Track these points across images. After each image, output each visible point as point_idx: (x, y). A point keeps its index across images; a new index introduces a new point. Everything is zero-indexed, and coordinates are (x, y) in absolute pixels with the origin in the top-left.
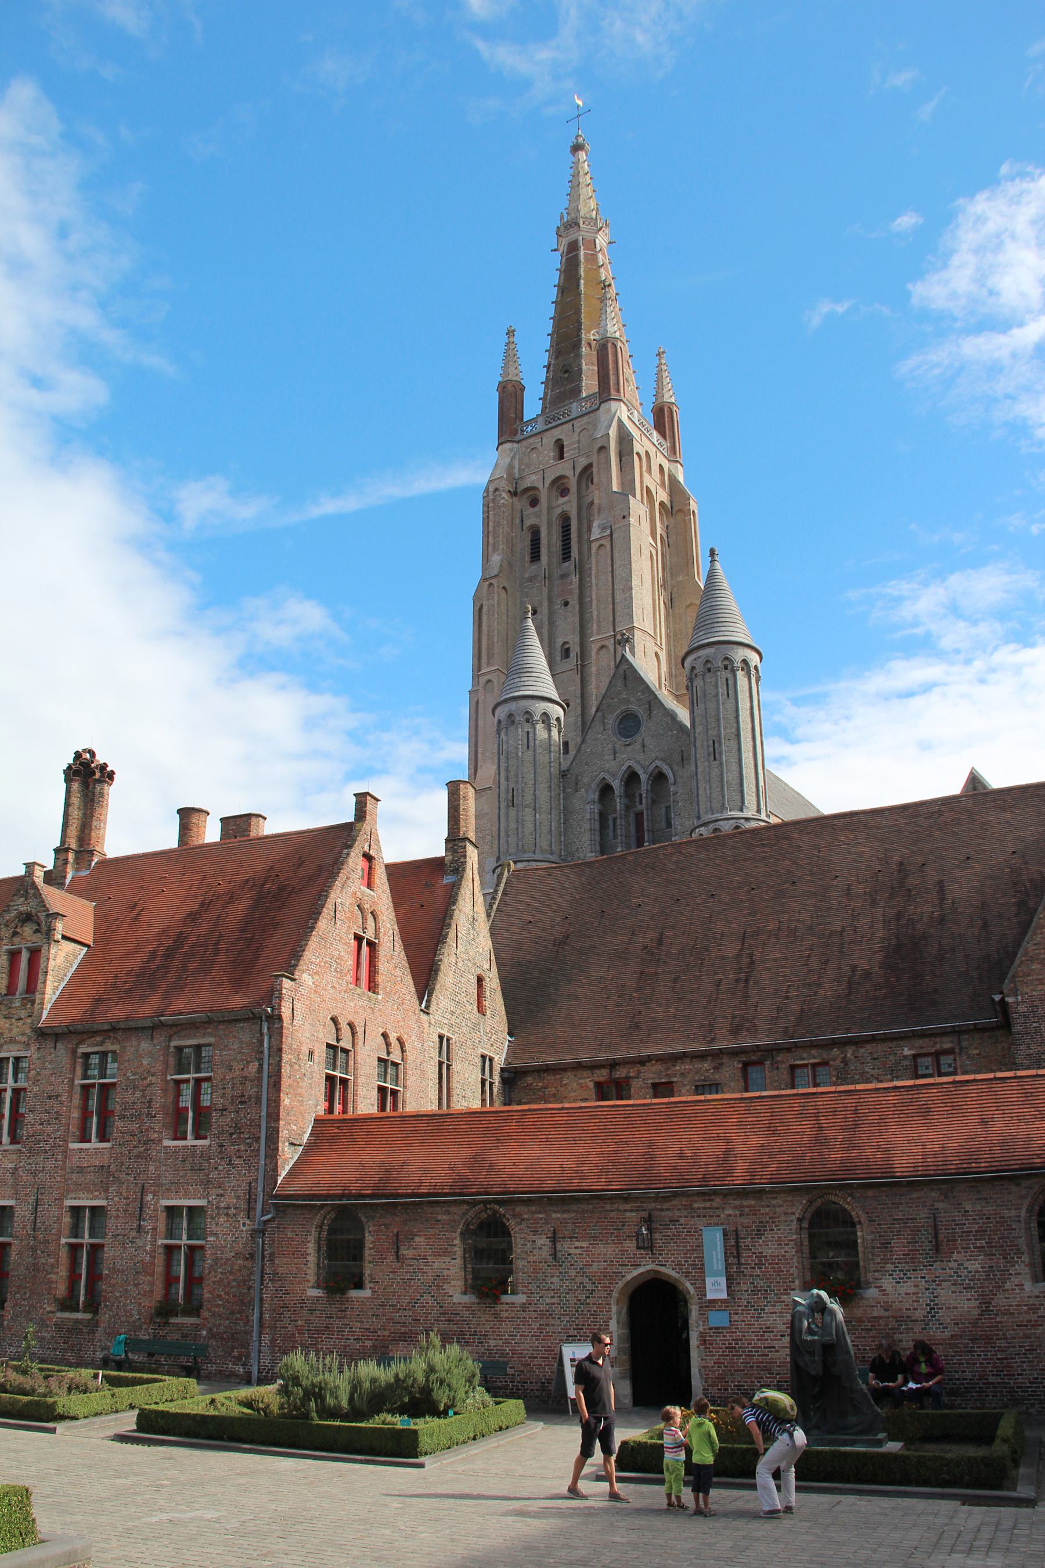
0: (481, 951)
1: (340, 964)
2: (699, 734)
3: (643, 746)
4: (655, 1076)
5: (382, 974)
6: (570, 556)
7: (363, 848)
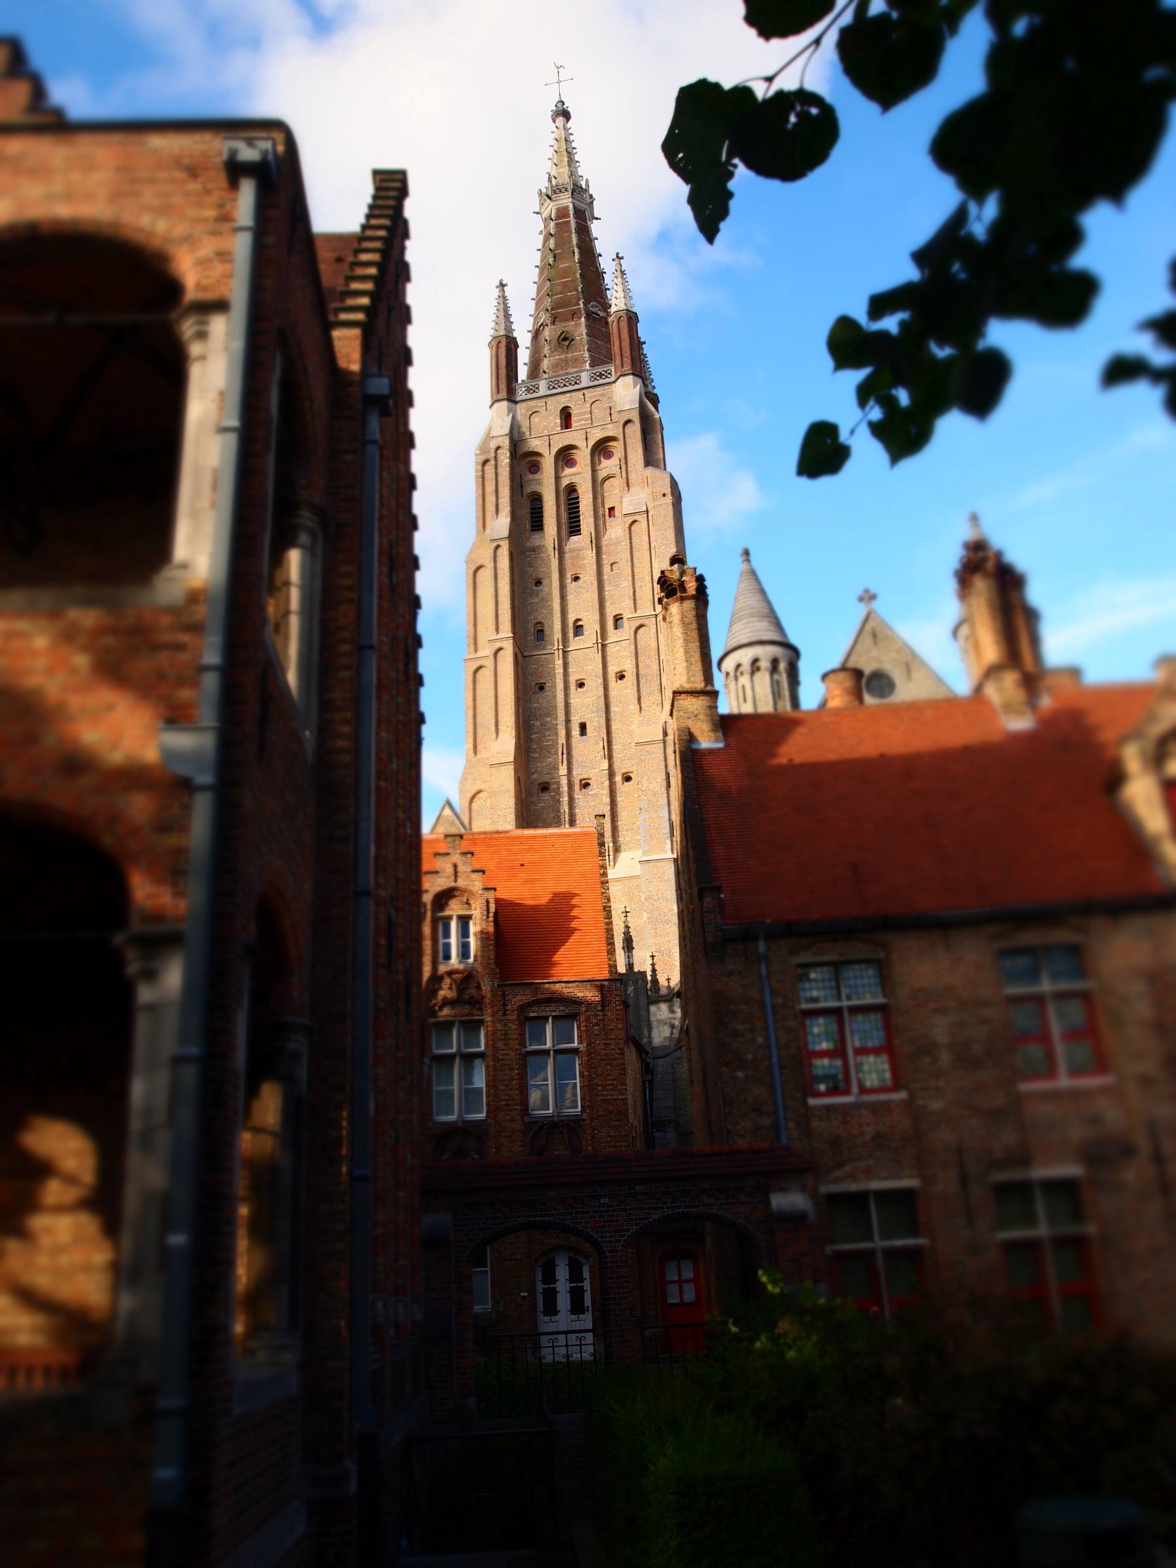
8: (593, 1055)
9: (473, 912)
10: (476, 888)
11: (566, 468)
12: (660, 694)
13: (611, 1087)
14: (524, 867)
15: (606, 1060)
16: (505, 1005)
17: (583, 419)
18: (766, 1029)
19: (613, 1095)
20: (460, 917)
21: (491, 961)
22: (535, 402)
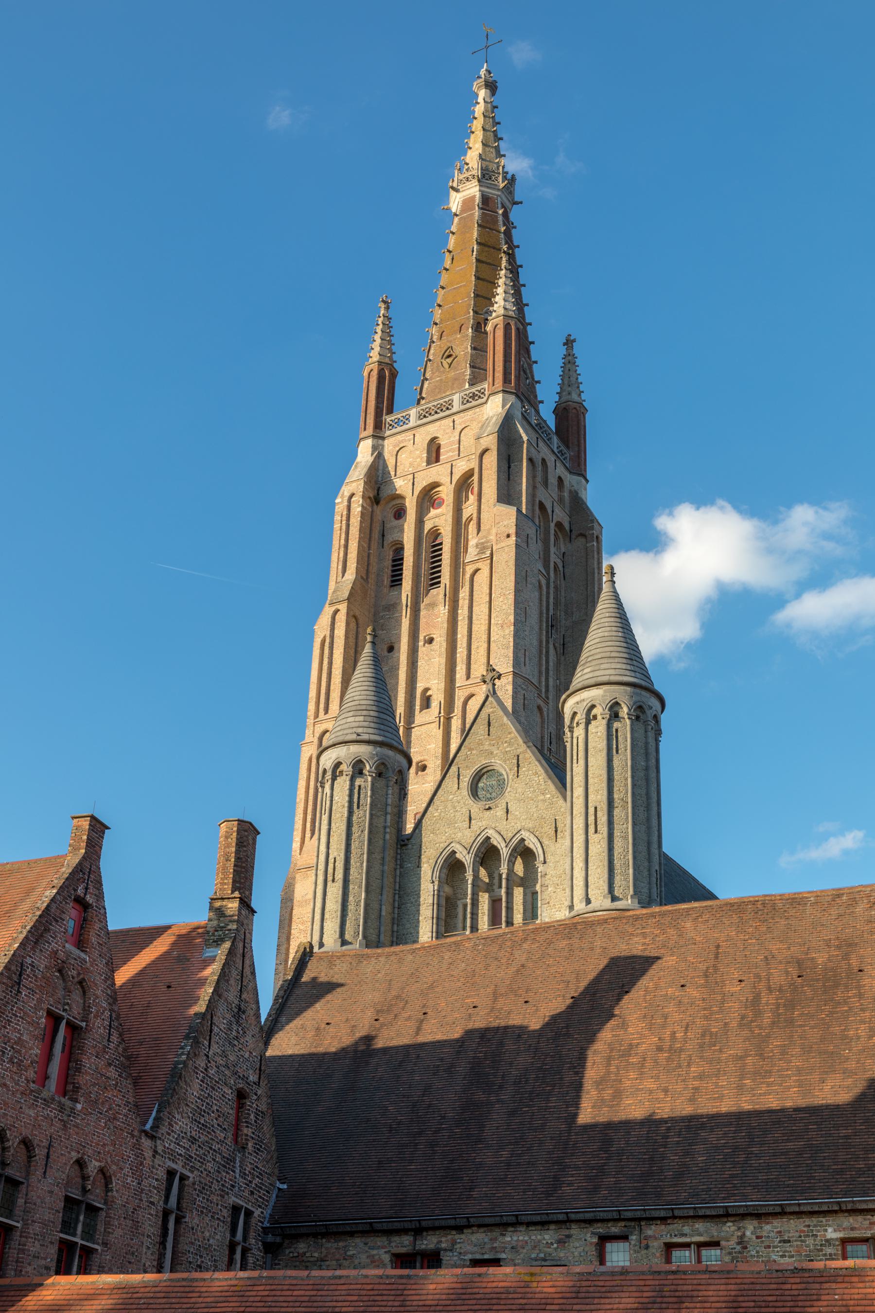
0: (247, 1055)
1: (19, 1052)
2: (578, 798)
3: (507, 812)
4: (475, 1249)
5: (87, 1073)
6: (439, 582)
7: (75, 890)
11: (432, 509)
17: (450, 451)
22: (403, 435)
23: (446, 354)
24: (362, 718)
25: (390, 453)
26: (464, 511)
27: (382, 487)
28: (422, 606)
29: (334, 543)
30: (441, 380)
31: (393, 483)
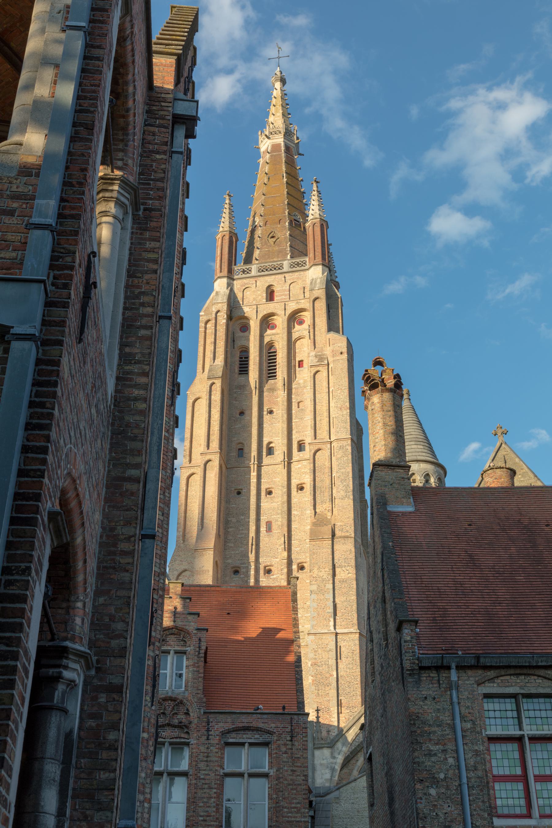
8: (281, 780)
9: (187, 649)
10: (192, 628)
12: (331, 503)
13: (295, 810)
14: (230, 615)
15: (292, 785)
16: (208, 730)
17: (283, 295)
18: (457, 751)
19: (296, 817)
20: (176, 652)
21: (199, 692)
23: (271, 235)
24: (422, 447)
25: (238, 289)
26: (293, 334)
27: (233, 310)
28: (265, 389)
29: (200, 340)
30: (269, 251)
31: (242, 309)
